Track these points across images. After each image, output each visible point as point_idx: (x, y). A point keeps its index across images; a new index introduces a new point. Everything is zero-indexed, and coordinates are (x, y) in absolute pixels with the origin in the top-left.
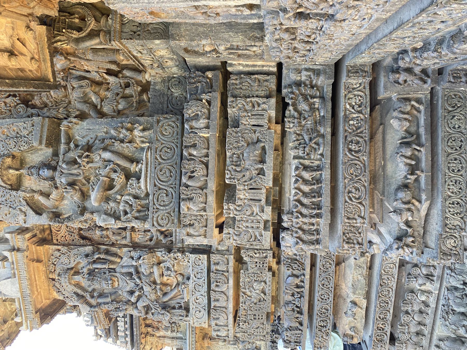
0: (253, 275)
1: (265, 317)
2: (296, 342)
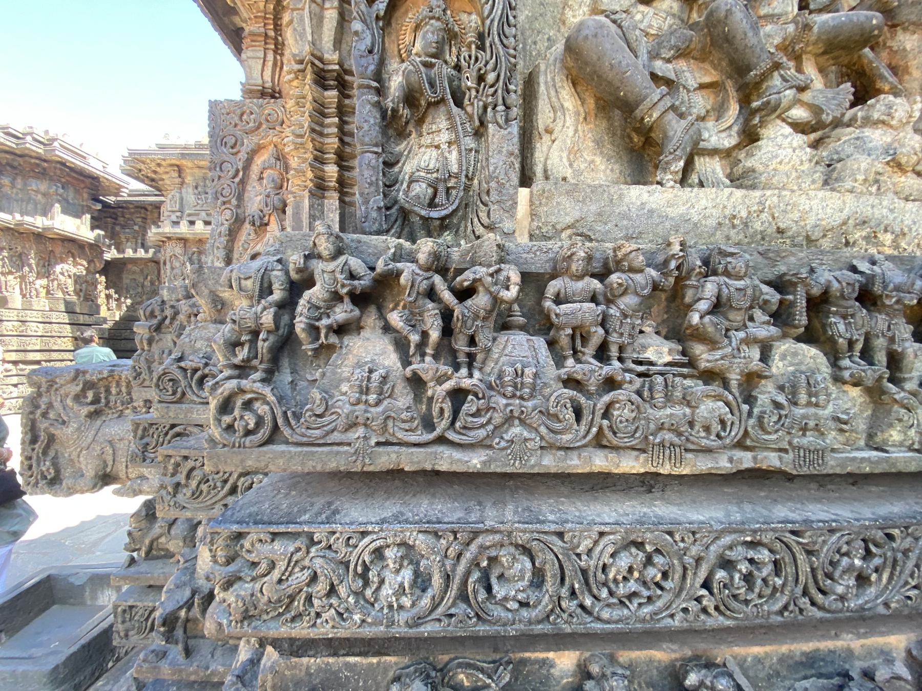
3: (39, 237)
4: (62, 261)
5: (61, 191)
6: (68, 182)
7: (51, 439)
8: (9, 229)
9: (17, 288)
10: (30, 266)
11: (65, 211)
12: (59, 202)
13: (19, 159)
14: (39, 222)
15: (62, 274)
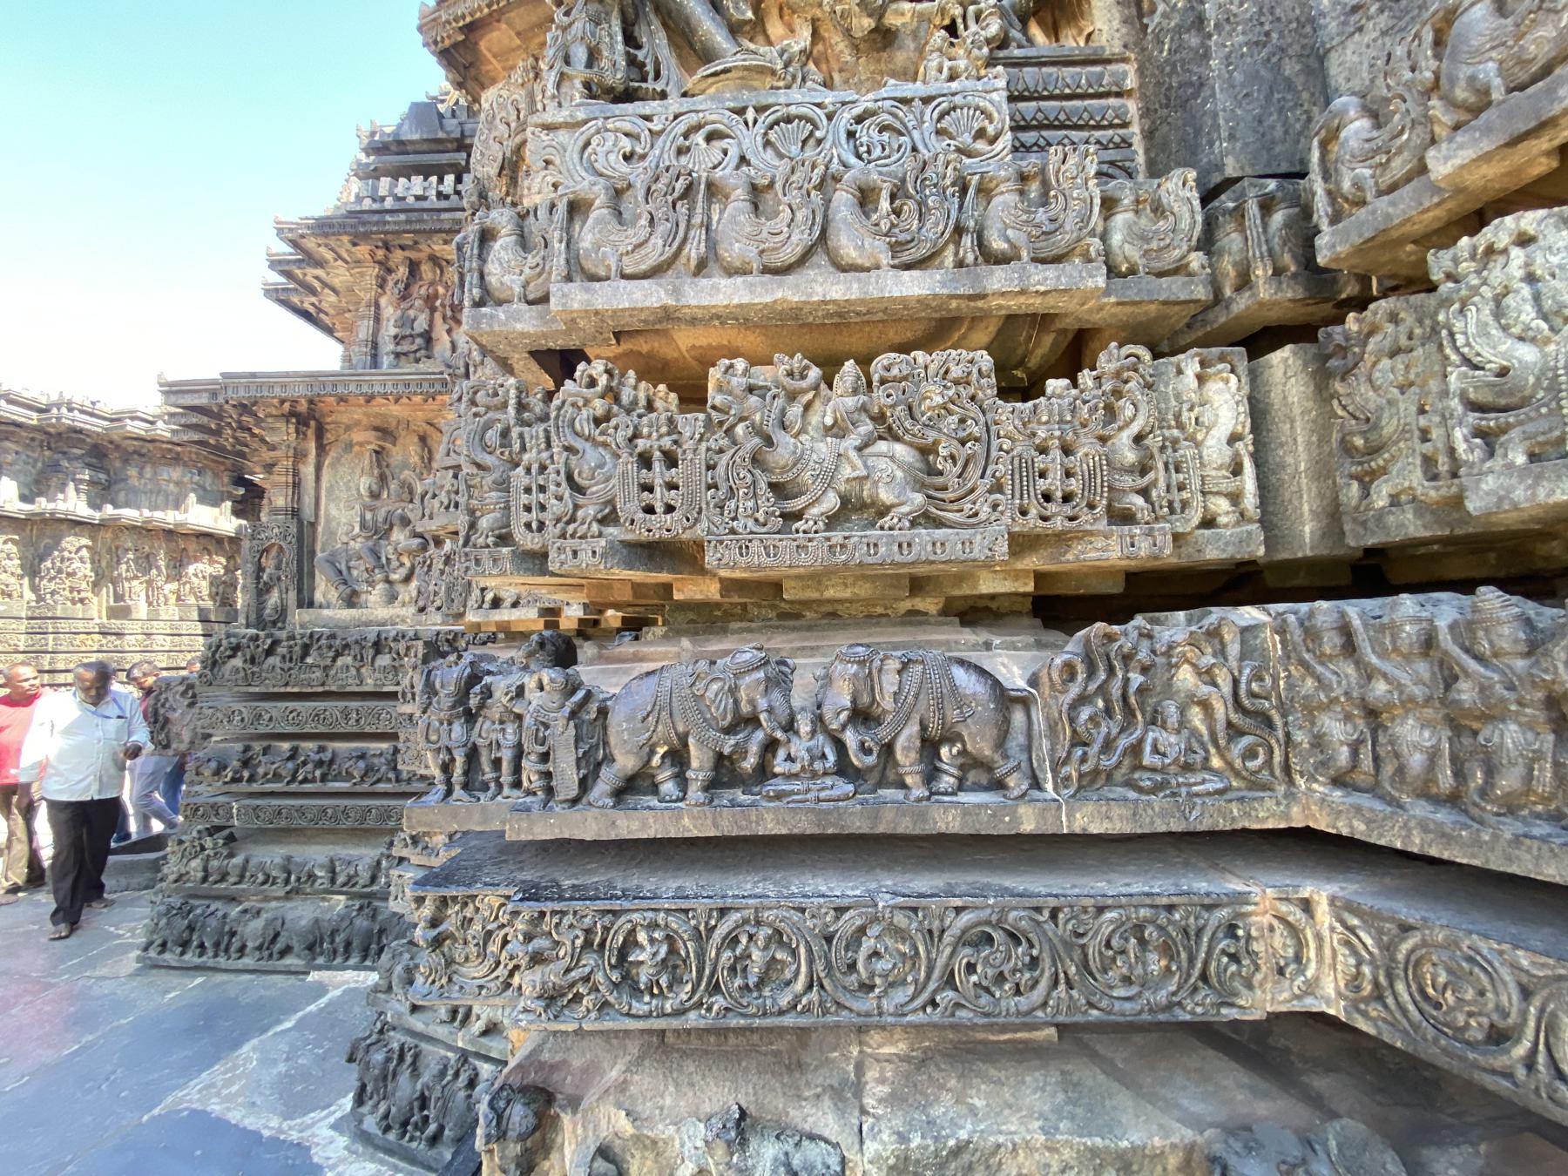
0: (976, 430)
1: (662, 527)
2: (473, 754)
3: (170, 534)
4: (196, 560)
5: (197, 478)
6: (206, 466)
7: (167, 720)
8: (134, 527)
10: (158, 568)
11: (201, 501)
12: (194, 490)
13: (150, 446)
14: (170, 517)
15: (196, 575)
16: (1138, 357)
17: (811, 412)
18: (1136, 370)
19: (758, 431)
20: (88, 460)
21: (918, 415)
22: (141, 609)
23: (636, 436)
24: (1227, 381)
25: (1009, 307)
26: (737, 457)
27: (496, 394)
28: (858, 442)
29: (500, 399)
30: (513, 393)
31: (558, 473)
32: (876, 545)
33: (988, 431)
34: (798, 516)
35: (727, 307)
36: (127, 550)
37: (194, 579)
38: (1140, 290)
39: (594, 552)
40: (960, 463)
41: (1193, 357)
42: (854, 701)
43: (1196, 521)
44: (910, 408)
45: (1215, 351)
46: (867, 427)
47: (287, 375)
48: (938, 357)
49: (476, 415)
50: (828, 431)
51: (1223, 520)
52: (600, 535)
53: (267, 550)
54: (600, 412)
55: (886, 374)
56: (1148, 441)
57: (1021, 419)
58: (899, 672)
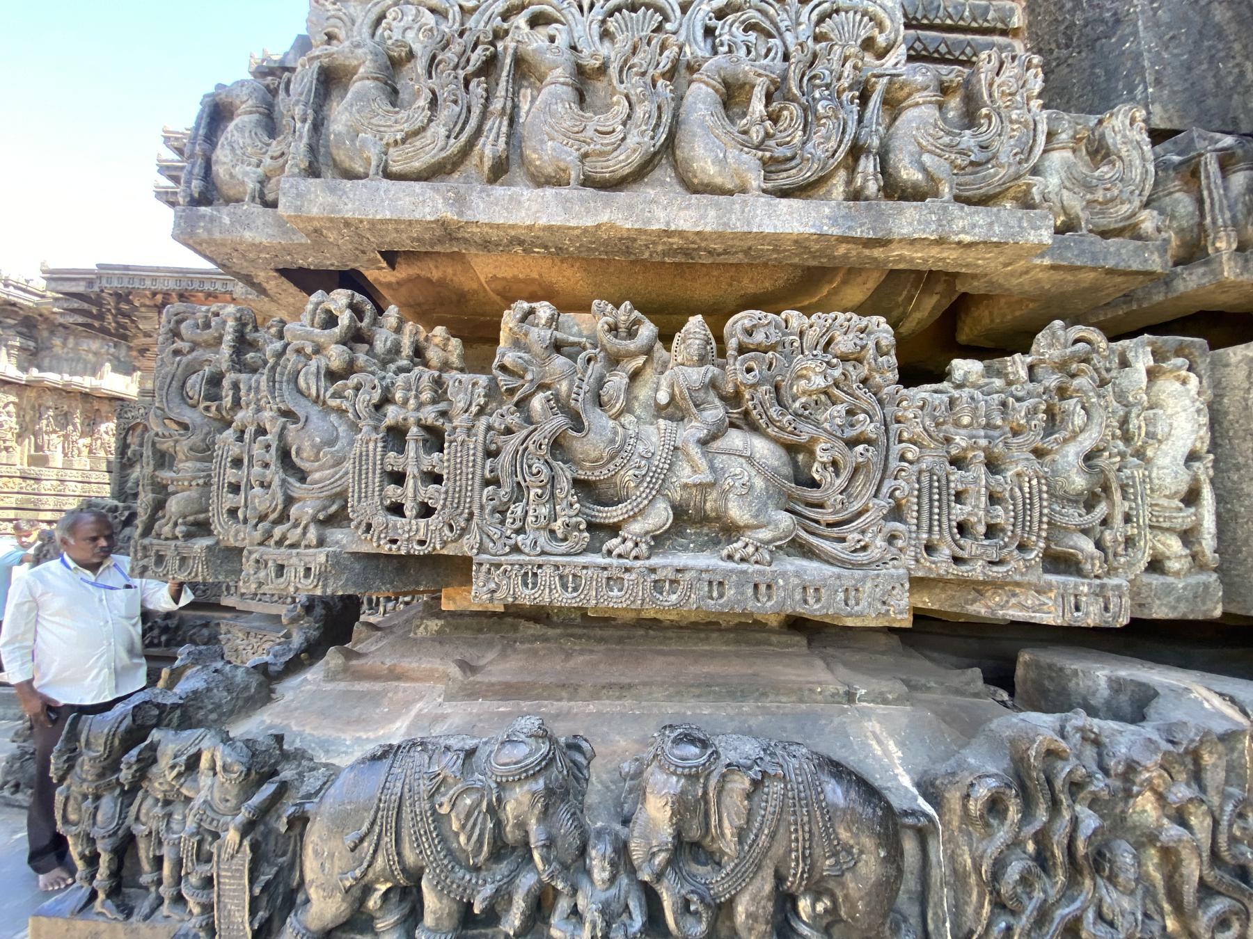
0: (870, 428)
5: (112, 350)
9: (60, 447)
10: (74, 425)
11: (115, 370)
12: (110, 361)
14: (86, 382)
15: (107, 433)
16: (1088, 342)
17: (640, 382)
18: (1086, 360)
19: (561, 405)
20: (20, 329)
21: (787, 400)
22: (57, 459)
23: (386, 400)
24: (1184, 382)
25: (912, 260)
26: (530, 443)
27: (207, 325)
28: (703, 434)
29: (211, 333)
30: (231, 323)
31: (268, 447)
32: (721, 584)
33: (887, 431)
34: (614, 530)
35: (530, 228)
36: (48, 408)
37: (105, 436)
38: (1083, 252)
39: (308, 570)
40: (845, 475)
41: (1143, 345)
42: (678, 835)
43: (1143, 565)
44: (777, 388)
45: (1172, 340)
46: (715, 412)
47: (158, 269)
48: (819, 320)
49: (177, 352)
50: (660, 411)
51: (1174, 565)
52: (321, 543)
53: (133, 428)
54: (336, 365)
55: (746, 340)
56: (1103, 461)
57: (934, 418)
58: (749, 796)
